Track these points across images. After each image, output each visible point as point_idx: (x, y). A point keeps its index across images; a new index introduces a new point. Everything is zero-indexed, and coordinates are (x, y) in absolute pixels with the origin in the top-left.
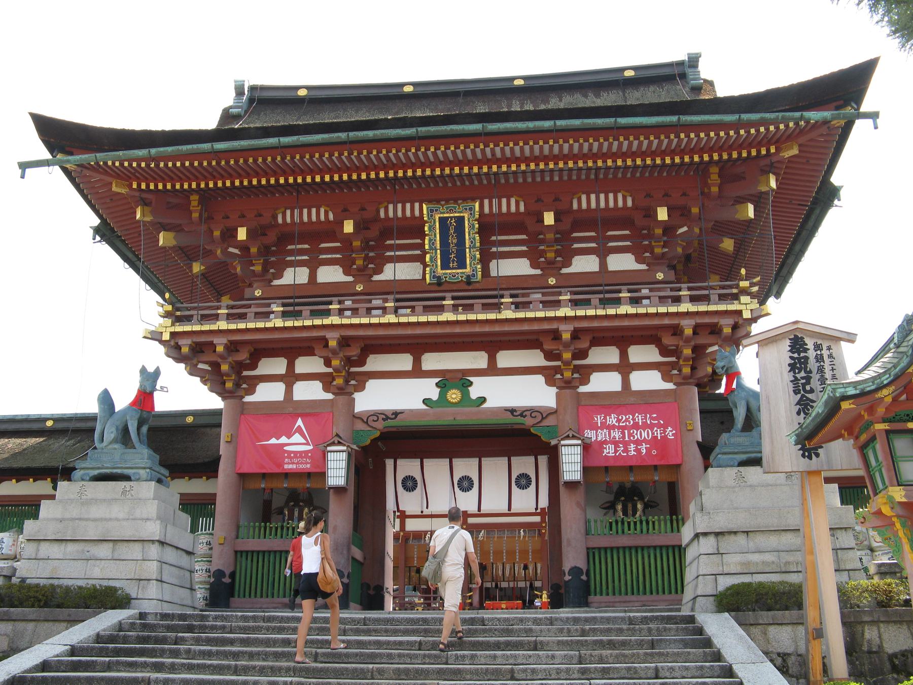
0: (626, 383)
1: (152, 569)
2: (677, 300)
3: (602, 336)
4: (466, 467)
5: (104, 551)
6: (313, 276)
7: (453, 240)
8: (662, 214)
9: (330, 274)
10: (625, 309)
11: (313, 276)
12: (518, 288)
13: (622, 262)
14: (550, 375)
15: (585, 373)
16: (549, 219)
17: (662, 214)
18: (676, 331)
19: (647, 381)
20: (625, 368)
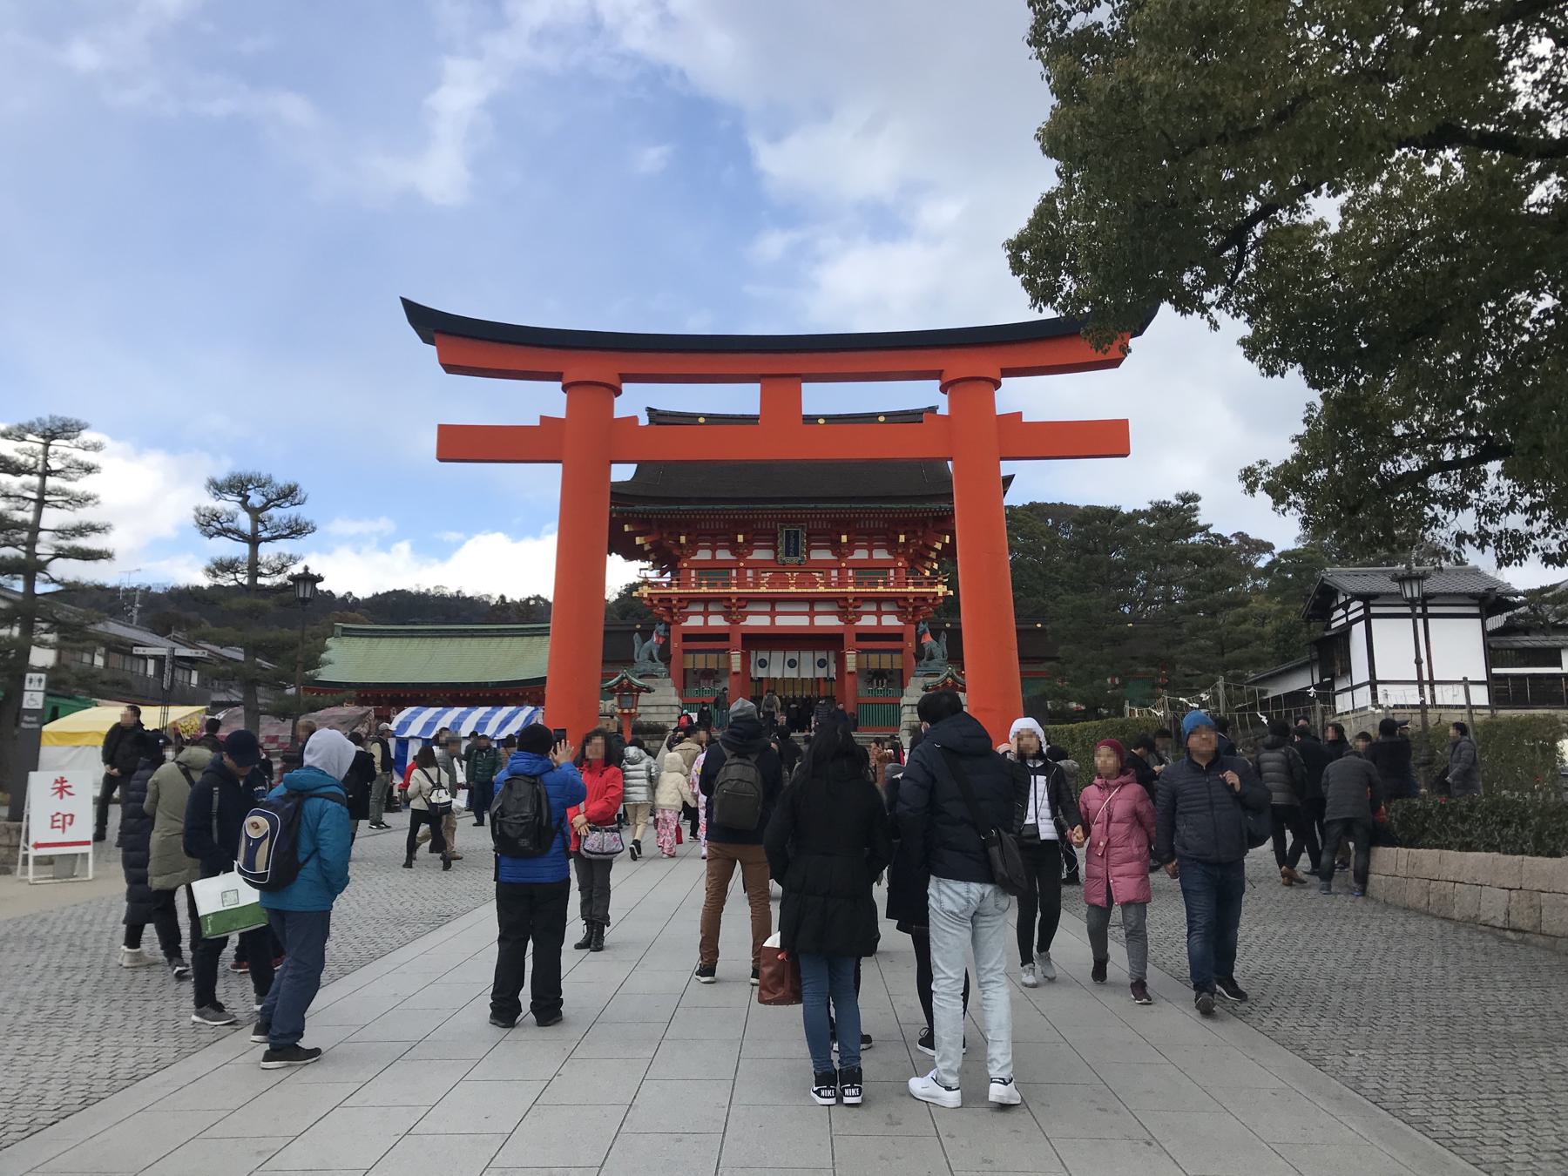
0: (879, 621)
1: (675, 717)
2: (907, 585)
3: (867, 599)
4: (793, 655)
5: (652, 710)
6: (714, 555)
7: (792, 541)
8: (902, 538)
9: (724, 555)
10: (881, 589)
11: (714, 555)
12: (824, 567)
13: (881, 555)
14: (842, 615)
15: (859, 616)
16: (844, 538)
17: (902, 538)
18: (906, 599)
19: (890, 621)
20: (879, 614)
